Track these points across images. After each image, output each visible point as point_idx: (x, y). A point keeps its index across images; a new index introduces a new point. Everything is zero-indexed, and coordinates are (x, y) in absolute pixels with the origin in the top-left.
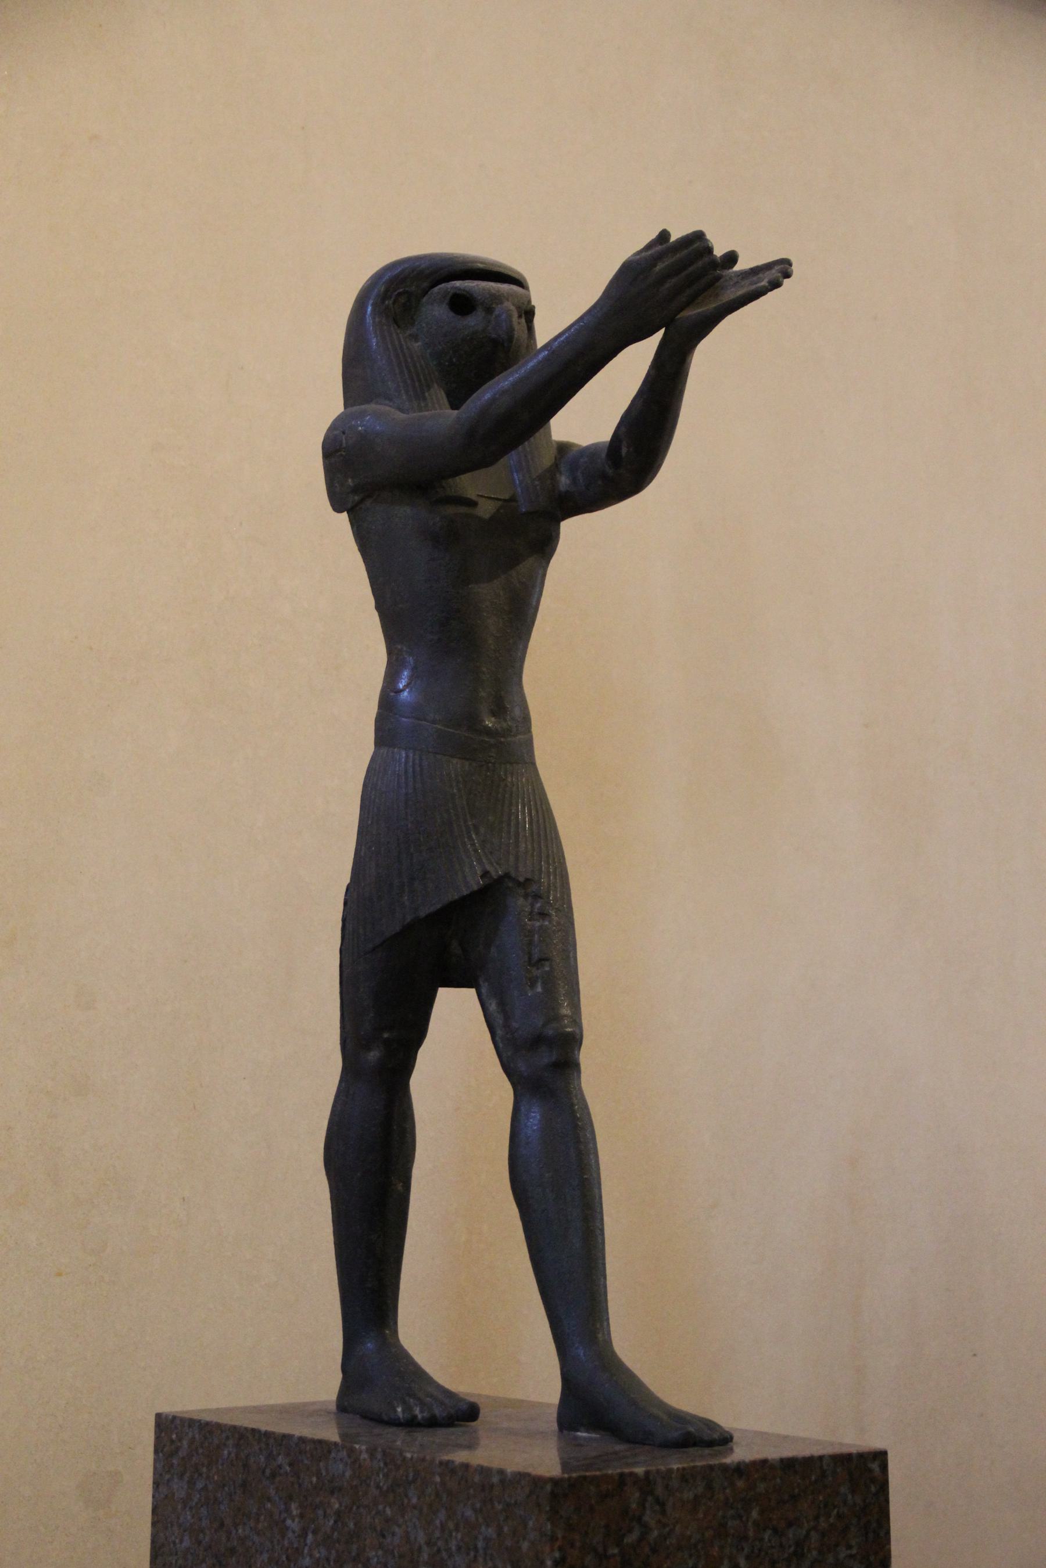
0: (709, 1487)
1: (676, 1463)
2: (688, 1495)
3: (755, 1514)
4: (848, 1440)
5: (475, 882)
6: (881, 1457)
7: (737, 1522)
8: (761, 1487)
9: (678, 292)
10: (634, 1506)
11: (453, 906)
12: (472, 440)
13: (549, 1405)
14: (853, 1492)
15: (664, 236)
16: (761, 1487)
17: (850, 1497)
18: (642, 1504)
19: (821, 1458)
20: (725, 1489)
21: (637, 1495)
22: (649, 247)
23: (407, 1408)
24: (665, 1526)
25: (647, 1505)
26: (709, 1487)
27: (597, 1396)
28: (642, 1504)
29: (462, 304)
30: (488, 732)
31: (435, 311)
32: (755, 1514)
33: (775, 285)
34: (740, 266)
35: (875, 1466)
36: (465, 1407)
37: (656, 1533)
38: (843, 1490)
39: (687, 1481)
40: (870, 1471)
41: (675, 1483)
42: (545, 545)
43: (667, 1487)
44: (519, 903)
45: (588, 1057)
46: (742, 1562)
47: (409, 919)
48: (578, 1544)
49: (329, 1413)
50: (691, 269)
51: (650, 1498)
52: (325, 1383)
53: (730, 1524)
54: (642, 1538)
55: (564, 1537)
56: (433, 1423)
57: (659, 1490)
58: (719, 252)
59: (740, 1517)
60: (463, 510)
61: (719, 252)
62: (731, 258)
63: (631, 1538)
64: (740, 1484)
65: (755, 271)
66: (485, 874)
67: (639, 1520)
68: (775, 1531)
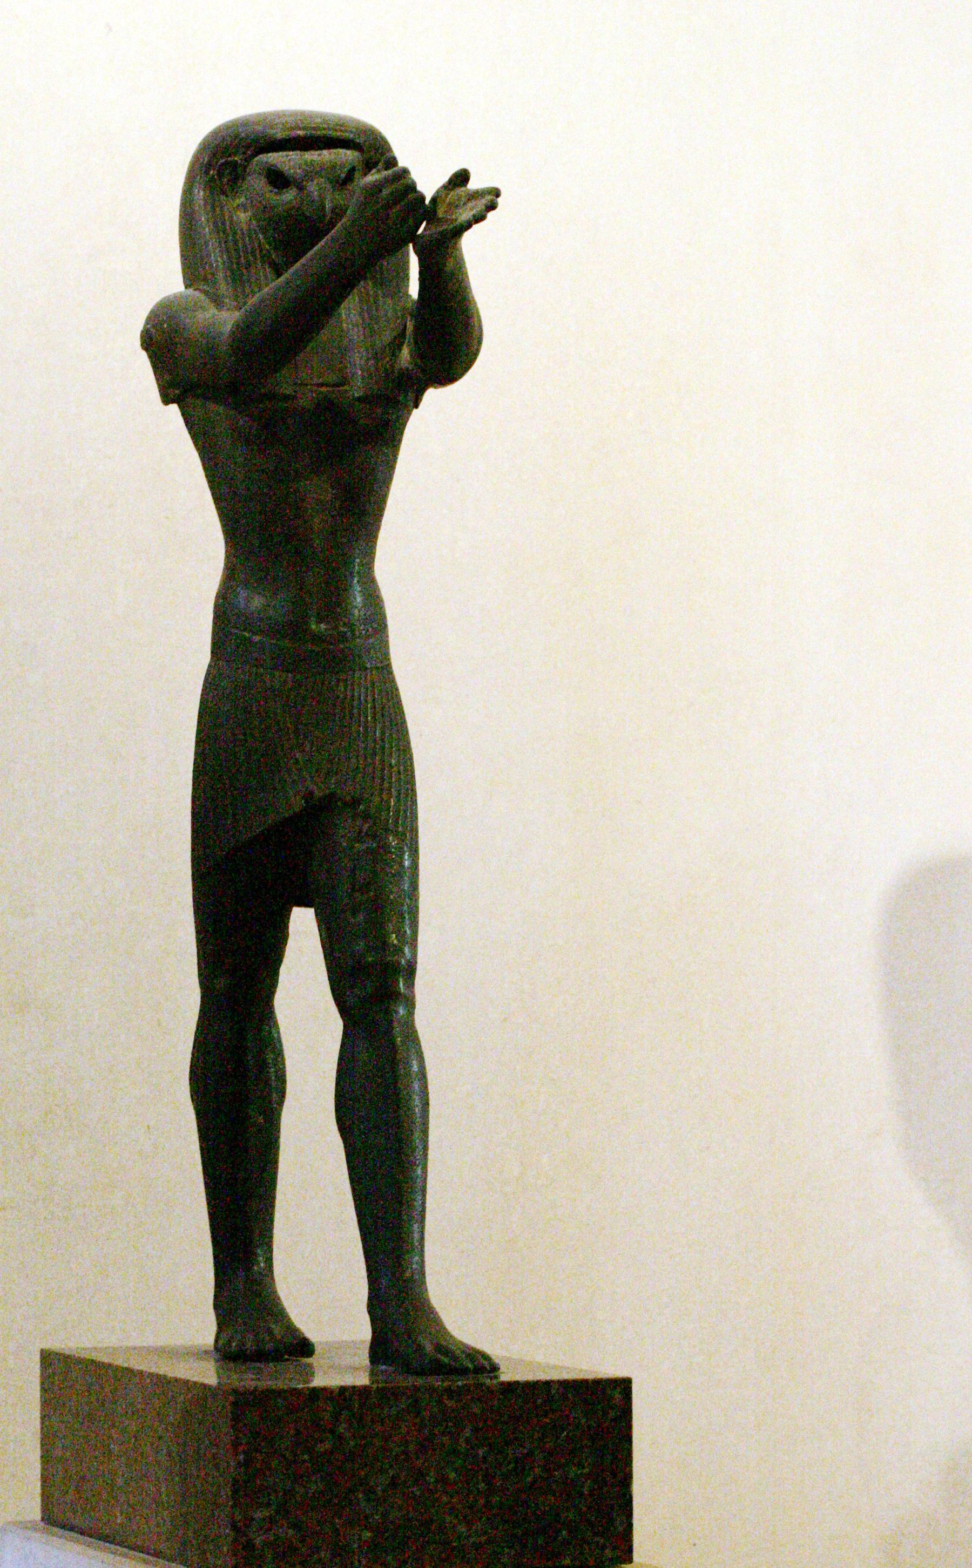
5: (298, 804)
6: (624, 1385)
12: (316, 309)
13: (363, 1342)
18: (336, 1417)
19: (548, 1383)
28: (336, 1417)
29: (278, 179)
30: (317, 638)
33: (479, 218)
34: (473, 185)
36: (289, 1340)
49: (206, 1352)
51: (345, 1413)
62: (461, 178)
67: (332, 1432)
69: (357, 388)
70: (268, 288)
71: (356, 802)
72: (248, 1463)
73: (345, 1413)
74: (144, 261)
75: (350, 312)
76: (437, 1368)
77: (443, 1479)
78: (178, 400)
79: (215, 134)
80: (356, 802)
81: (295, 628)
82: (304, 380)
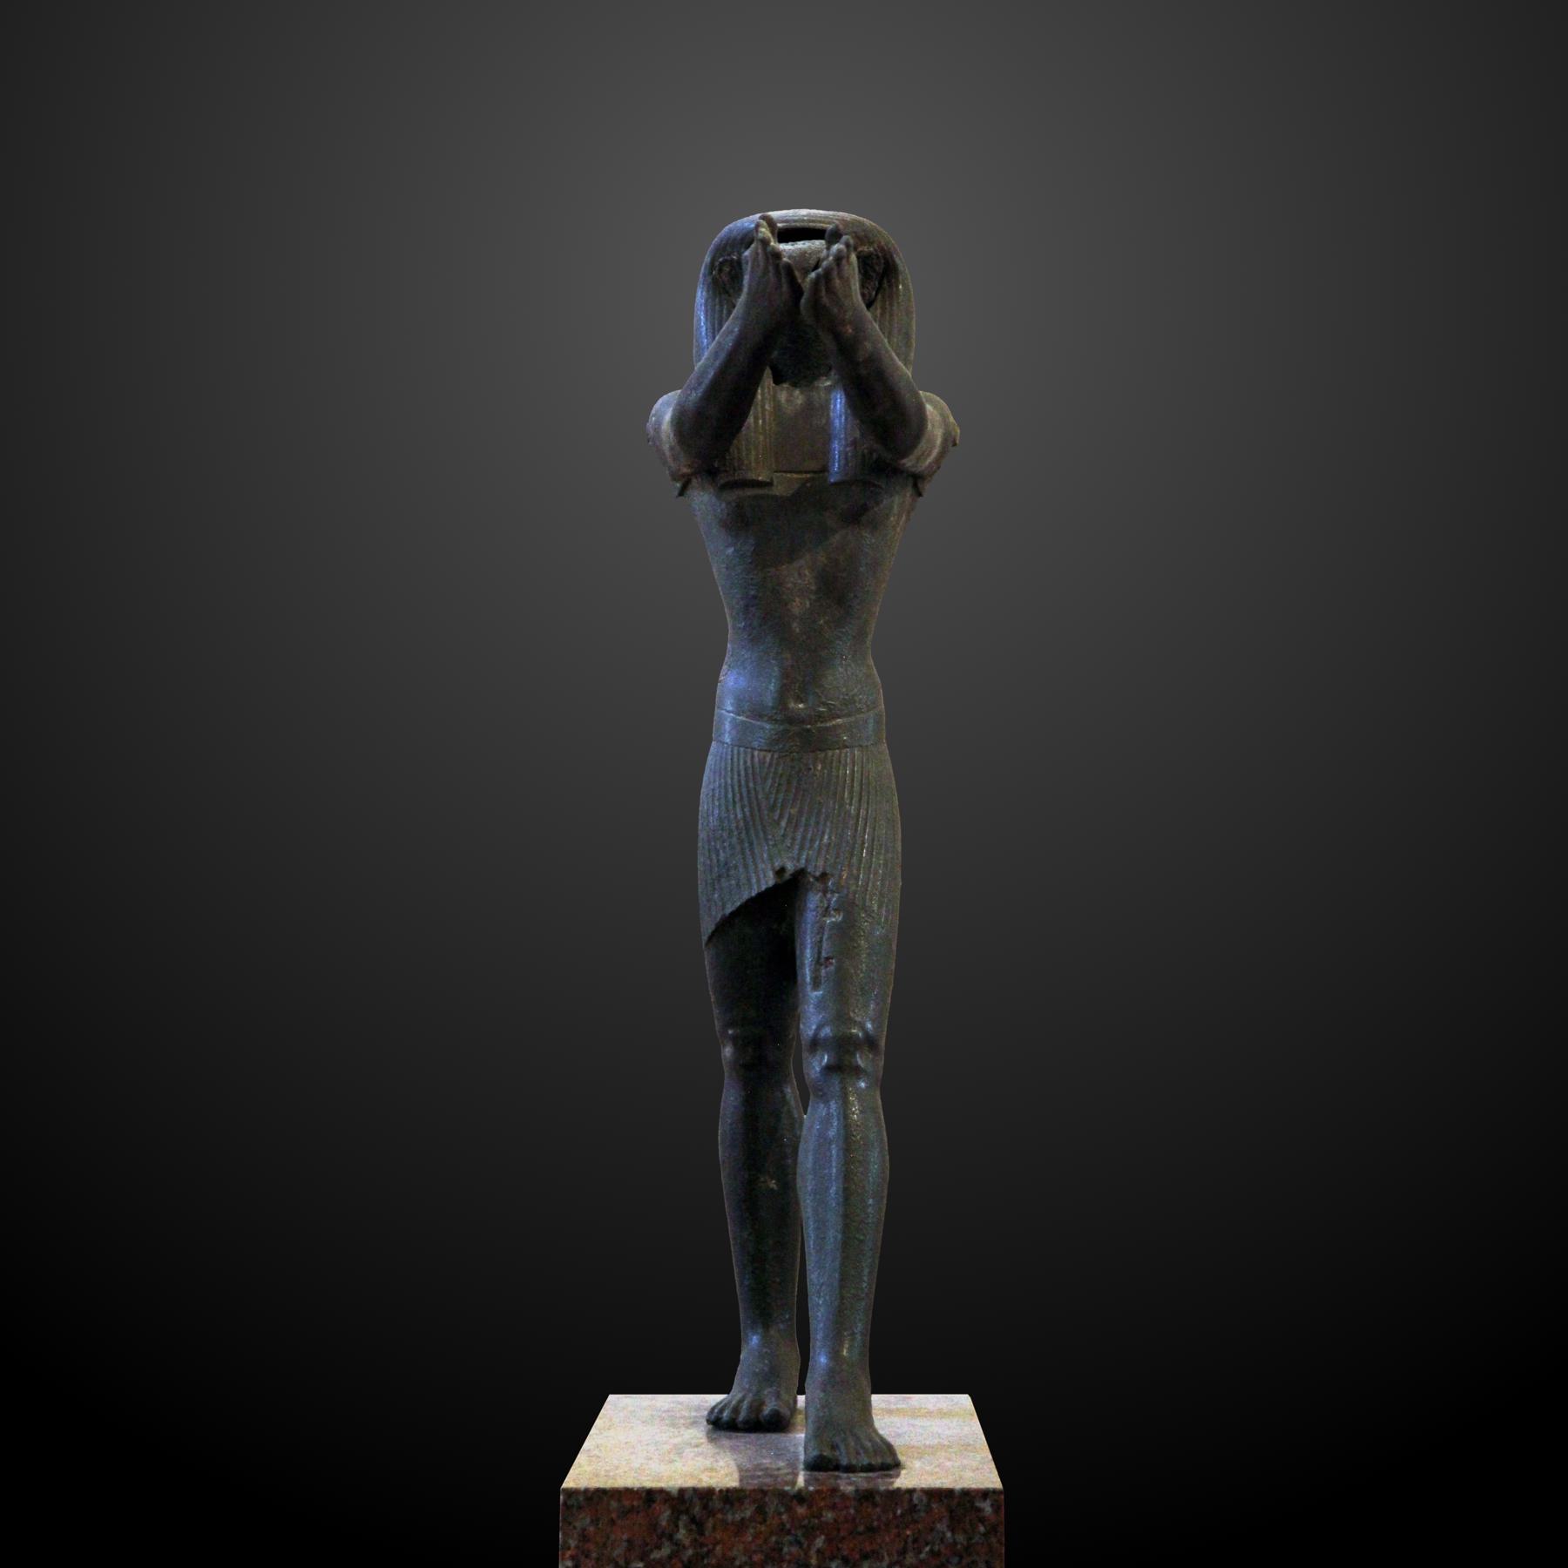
0: (761, 1510)
2: (733, 1516)
3: (820, 1542)
4: (968, 1474)
5: (769, 880)
7: (794, 1549)
8: (829, 1516)
10: (664, 1523)
14: (953, 1531)
17: (949, 1535)
20: (780, 1514)
21: (668, 1513)
24: (702, 1545)
25: (681, 1524)
26: (761, 1510)
32: (820, 1542)
37: (690, 1552)
39: (732, 1504)
40: (979, 1510)
41: (716, 1504)
43: (705, 1507)
48: (594, 1555)
51: (684, 1517)
53: (786, 1550)
54: (674, 1555)
55: (577, 1547)
57: (697, 1510)
59: (799, 1543)
60: (750, 492)
64: (801, 1510)
66: (780, 872)
67: (670, 1537)
80: (824, 877)
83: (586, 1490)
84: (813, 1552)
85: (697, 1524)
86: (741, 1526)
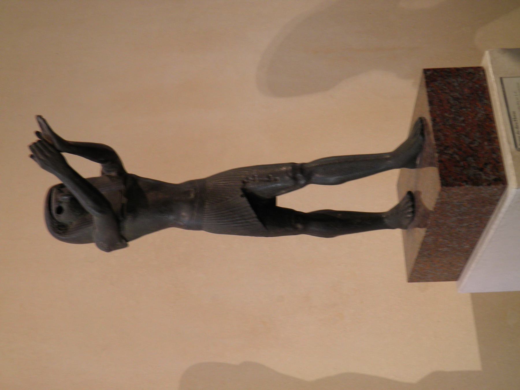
0: (439, 131)
1: (431, 138)
2: (442, 138)
3: (446, 115)
5: (244, 199)
6: (426, 71)
8: (438, 112)
9: (50, 149)
11: (252, 204)
15: (32, 156)
16: (438, 112)
19: (428, 92)
21: (444, 156)
22: (35, 160)
23: (409, 213)
25: (447, 152)
26: (439, 131)
27: (406, 157)
29: (60, 210)
31: (62, 218)
32: (446, 115)
33: (44, 121)
34: (39, 129)
35: (429, 73)
38: (436, 84)
42: (135, 179)
44: (251, 186)
45: (299, 161)
46: (462, 119)
47: (257, 219)
50: (42, 148)
52: (398, 233)
54: (457, 154)
56: (413, 206)
57: (442, 148)
58: (35, 139)
61: (35, 139)
62: (38, 133)
63: (457, 157)
64: (438, 120)
65: (41, 125)
66: (242, 196)
67: (451, 155)
68: (451, 108)
69: (122, 187)
70: (96, 217)
71: (244, 182)
72: (466, 181)
73: (445, 152)
74: (87, 254)
75: (104, 192)
76: (422, 134)
77: (463, 121)
78: (127, 241)
79: (50, 231)
80: (244, 182)
81: (192, 203)
82: (117, 200)
83: (441, 180)
84: (450, 116)
85: (447, 147)
86: (445, 135)
